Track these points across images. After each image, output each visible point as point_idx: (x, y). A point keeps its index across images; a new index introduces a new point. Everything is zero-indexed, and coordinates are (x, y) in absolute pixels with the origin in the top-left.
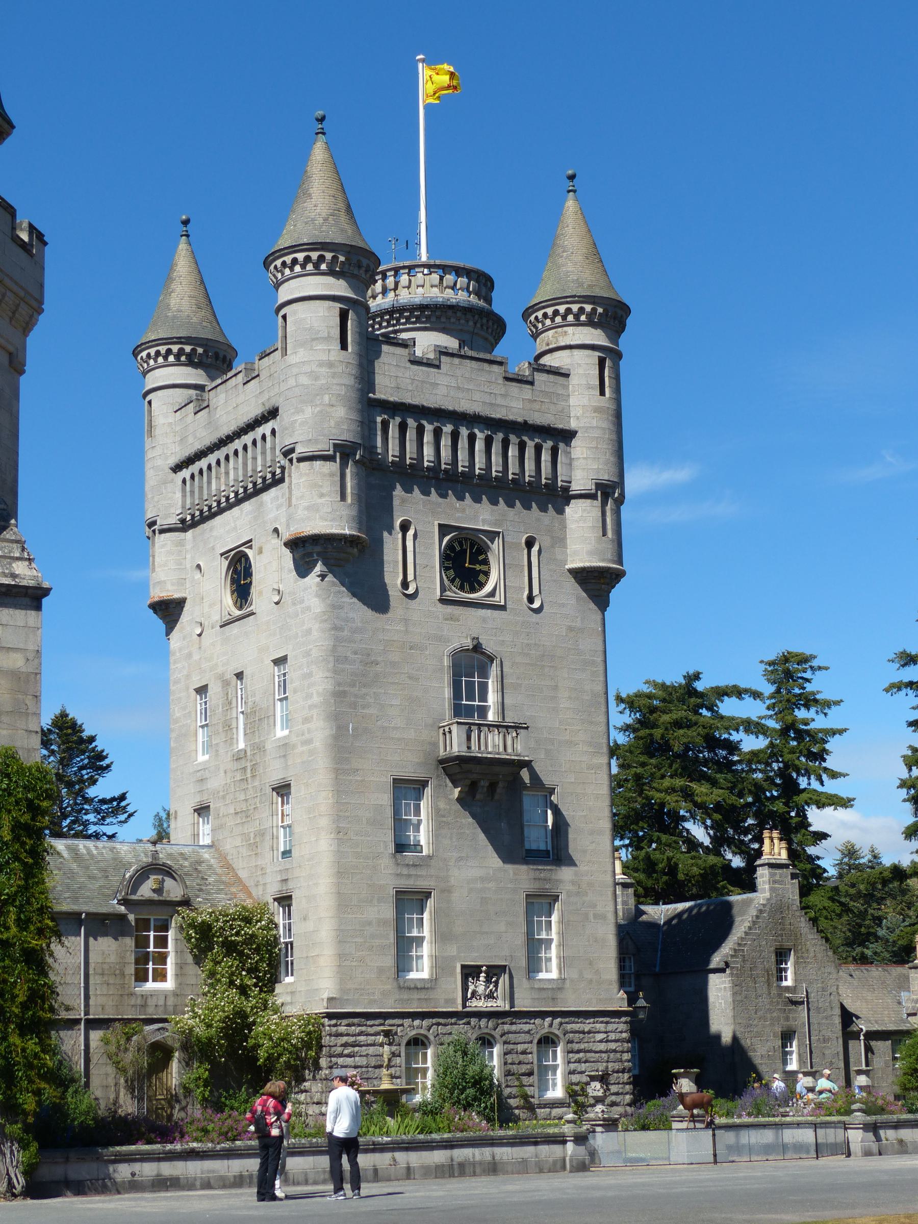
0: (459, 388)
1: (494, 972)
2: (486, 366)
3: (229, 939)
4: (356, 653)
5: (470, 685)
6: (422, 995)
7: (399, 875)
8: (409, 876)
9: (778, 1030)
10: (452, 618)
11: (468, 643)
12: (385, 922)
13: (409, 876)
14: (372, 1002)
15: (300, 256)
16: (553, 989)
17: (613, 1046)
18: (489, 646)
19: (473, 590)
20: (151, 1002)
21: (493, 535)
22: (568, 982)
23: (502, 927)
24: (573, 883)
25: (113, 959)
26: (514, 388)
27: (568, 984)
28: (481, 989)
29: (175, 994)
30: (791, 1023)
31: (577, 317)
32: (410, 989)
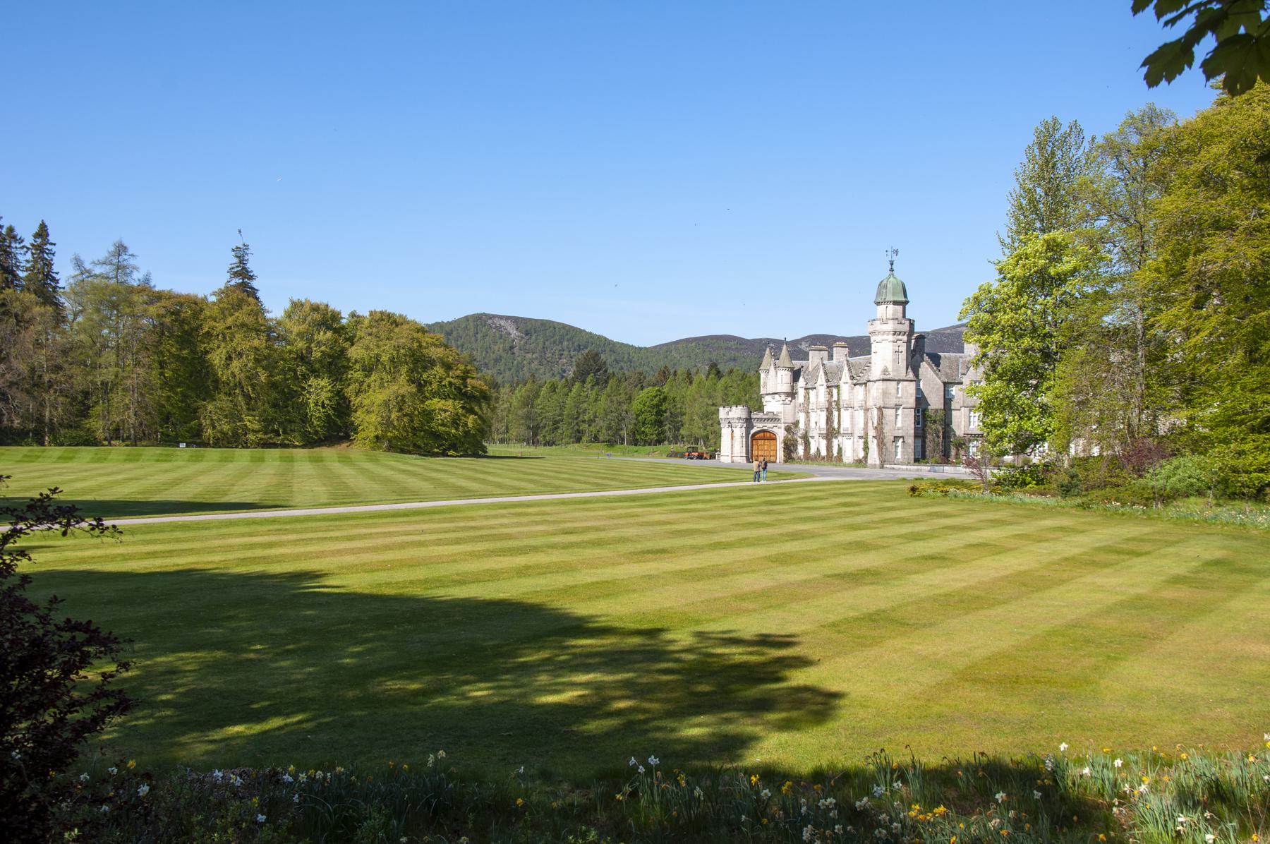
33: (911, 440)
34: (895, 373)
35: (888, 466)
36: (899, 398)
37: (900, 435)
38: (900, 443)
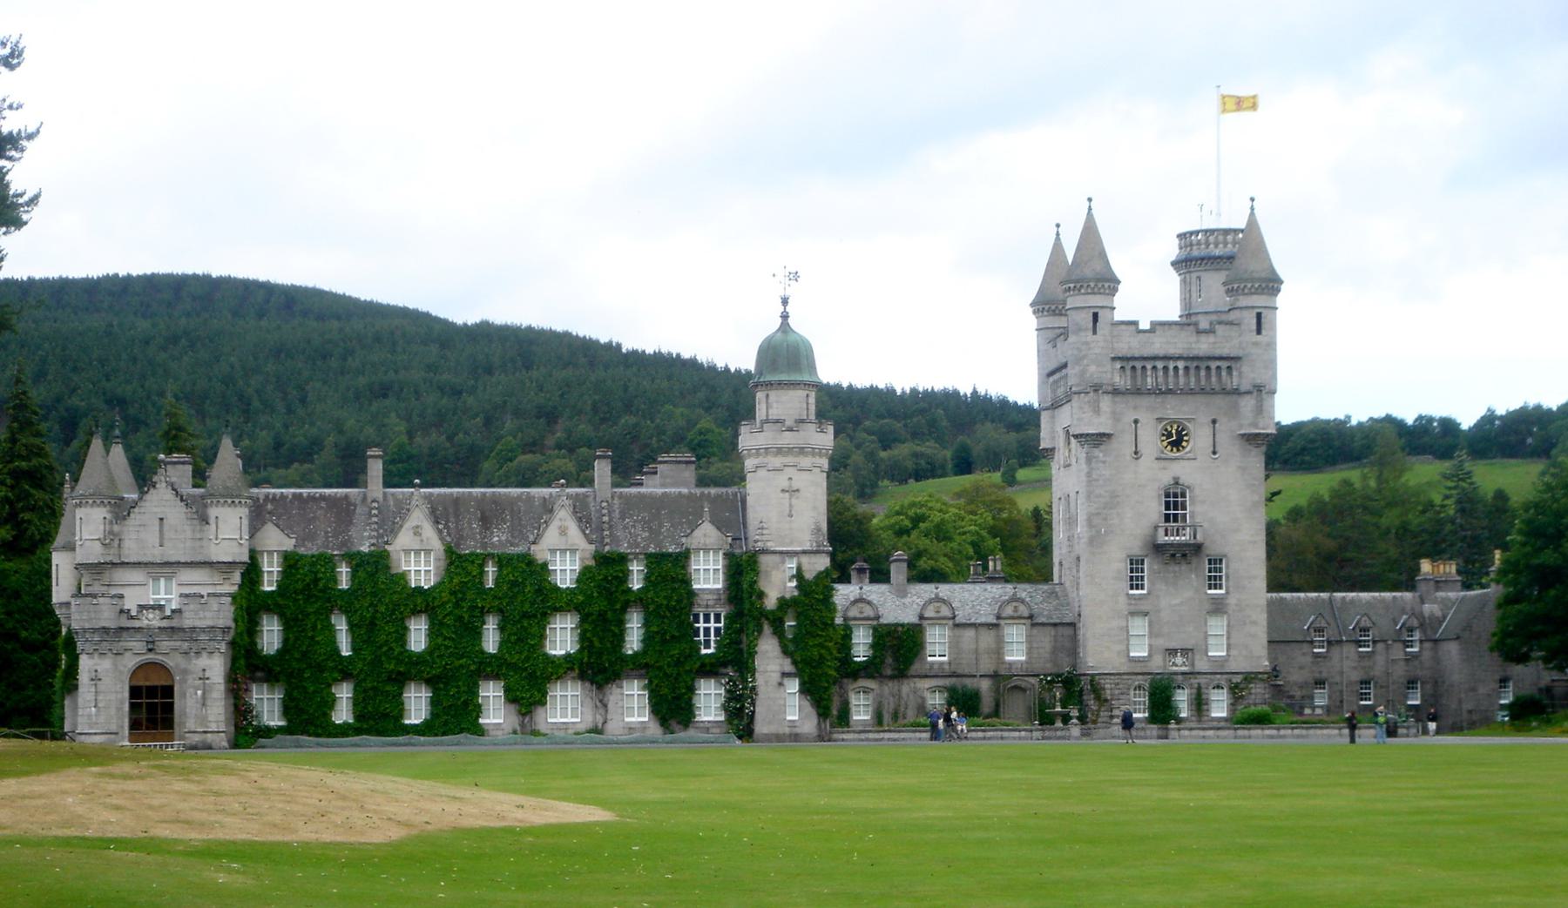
1: (1185, 652)
2: (1186, 327)
3: (1451, 568)
5: (1176, 503)
6: (1143, 664)
7: (1131, 604)
9: (1497, 677)
10: (1164, 469)
11: (1172, 482)
12: (1122, 629)
13: (1136, 605)
14: (1113, 668)
15: (1072, 285)
17: (1258, 690)
18: (1185, 480)
19: (1178, 450)
20: (1014, 667)
21: (1189, 420)
23: (1191, 629)
24: (1236, 605)
25: (993, 646)
26: (1203, 338)
27: (1231, 658)
28: (1177, 662)
29: (1026, 662)
30: (1509, 673)
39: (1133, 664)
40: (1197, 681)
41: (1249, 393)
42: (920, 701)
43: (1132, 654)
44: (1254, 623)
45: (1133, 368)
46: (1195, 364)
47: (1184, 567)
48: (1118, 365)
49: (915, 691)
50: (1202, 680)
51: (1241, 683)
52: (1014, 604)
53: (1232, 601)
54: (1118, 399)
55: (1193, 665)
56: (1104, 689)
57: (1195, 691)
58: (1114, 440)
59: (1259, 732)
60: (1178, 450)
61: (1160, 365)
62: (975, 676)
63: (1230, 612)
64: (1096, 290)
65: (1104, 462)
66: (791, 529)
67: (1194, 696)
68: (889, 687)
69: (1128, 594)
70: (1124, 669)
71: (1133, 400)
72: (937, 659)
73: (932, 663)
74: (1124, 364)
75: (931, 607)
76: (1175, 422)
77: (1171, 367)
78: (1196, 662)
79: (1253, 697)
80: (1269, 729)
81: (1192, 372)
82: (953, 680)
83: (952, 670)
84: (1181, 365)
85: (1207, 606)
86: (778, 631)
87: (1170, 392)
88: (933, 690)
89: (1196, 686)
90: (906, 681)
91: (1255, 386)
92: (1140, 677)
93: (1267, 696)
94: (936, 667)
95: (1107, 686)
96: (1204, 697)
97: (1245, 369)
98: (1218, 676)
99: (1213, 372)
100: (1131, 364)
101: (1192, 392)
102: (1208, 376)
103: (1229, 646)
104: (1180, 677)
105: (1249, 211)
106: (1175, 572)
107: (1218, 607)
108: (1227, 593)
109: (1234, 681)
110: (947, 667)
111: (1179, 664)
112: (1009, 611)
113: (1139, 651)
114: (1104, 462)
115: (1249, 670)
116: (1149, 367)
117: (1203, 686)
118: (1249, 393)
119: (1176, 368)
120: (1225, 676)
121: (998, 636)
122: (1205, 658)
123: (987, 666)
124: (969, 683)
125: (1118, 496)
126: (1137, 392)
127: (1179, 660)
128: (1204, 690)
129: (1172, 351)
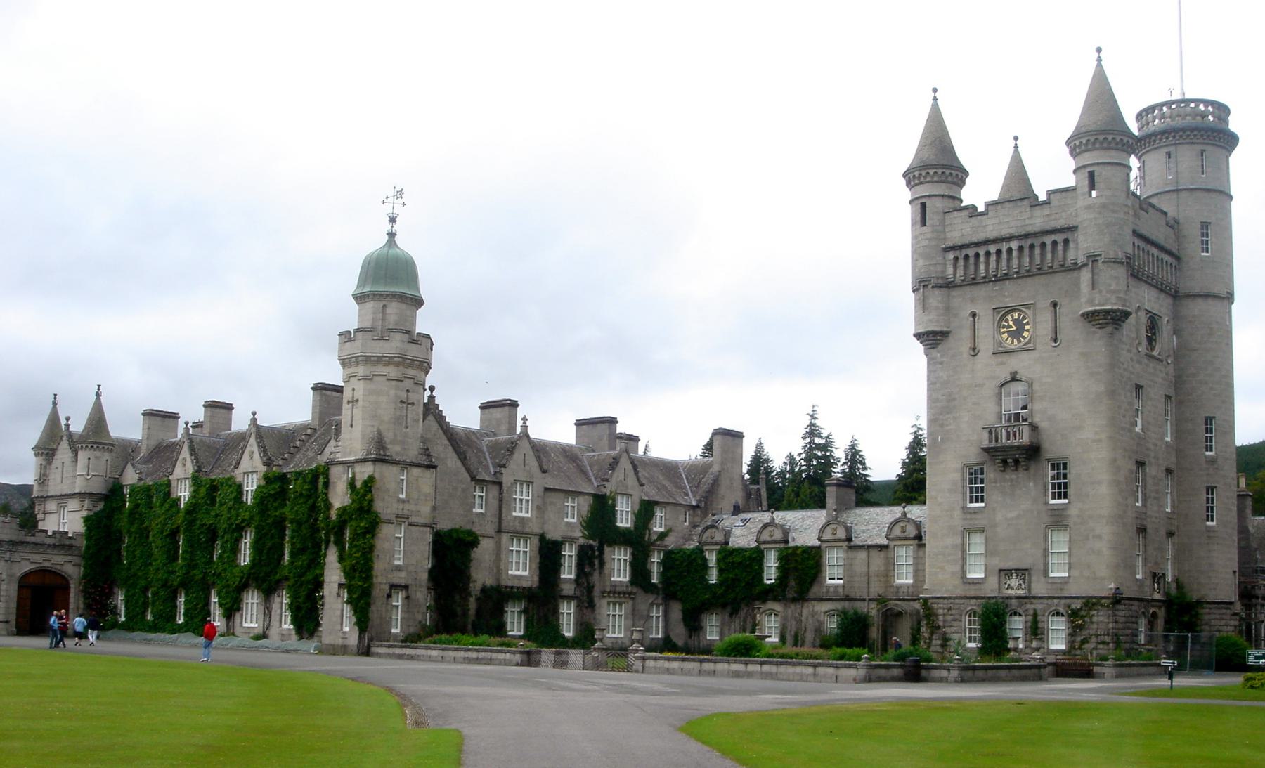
0: (1000, 223)
1: (1022, 572)
2: (1019, 203)
4: (943, 395)
6: (977, 587)
7: (964, 519)
8: (971, 519)
10: (1002, 363)
13: (971, 519)
16: (1061, 583)
17: (1101, 619)
20: (901, 590)
22: (1072, 578)
24: (1079, 516)
26: (1038, 212)
28: (1012, 585)
29: (912, 585)
31: (1101, 143)
32: (969, 583)
33: (423, 596)
34: (397, 448)
35: (380, 650)
36: (403, 501)
37: (403, 582)
38: (398, 601)
39: (967, 587)
40: (1032, 606)
41: (1085, 265)
42: (817, 624)
43: (970, 576)
44: (1099, 537)
45: (967, 257)
46: (1029, 241)
47: (1022, 474)
48: (951, 256)
49: (814, 614)
50: (1039, 606)
51: (1081, 609)
52: (902, 524)
53: (1073, 511)
54: (955, 293)
55: (1030, 591)
56: (937, 615)
57: (1030, 618)
58: (951, 338)
59: (726, 666)
60: (1019, 341)
61: (993, 249)
62: (864, 600)
63: (1071, 525)
64: (922, 180)
65: (941, 363)
66: (351, 439)
67: (1029, 624)
68: (793, 609)
69: (964, 508)
70: (959, 592)
71: (969, 292)
72: (836, 582)
73: (829, 587)
74: (957, 253)
75: (829, 530)
76: (1015, 310)
77: (1004, 250)
78: (1033, 585)
79: (1095, 626)
80: (735, 662)
81: (1026, 251)
82: (846, 604)
83: (846, 593)
84: (1014, 245)
85: (1046, 519)
86: (340, 543)
87: (1007, 277)
88: (830, 613)
89: (1031, 612)
90: (806, 604)
91: (1089, 257)
92: (973, 601)
93: (1111, 625)
94: (832, 589)
95: (941, 611)
96: (1040, 625)
97: (1081, 238)
98: (1056, 601)
99: (1049, 248)
100: (964, 252)
101: (1029, 275)
102: (1043, 255)
103: (1070, 568)
104: (1014, 602)
105: (1095, 63)
106: (1012, 480)
107: (1058, 520)
108: (1069, 502)
109: (1073, 607)
110: (841, 590)
111: (1015, 587)
112: (897, 532)
113: (976, 573)
114: (941, 363)
115: (1091, 593)
116: (982, 253)
117: (1039, 612)
118: (1085, 265)
119: (1010, 250)
120: (1063, 601)
121: (887, 558)
122: (1043, 579)
123: (876, 589)
124: (862, 607)
125: (954, 399)
126: (974, 282)
127: (1014, 582)
128: (1039, 618)
129: (1005, 232)
